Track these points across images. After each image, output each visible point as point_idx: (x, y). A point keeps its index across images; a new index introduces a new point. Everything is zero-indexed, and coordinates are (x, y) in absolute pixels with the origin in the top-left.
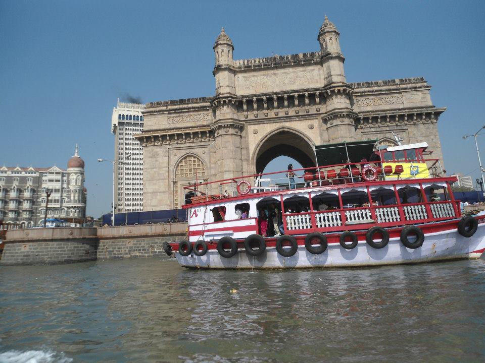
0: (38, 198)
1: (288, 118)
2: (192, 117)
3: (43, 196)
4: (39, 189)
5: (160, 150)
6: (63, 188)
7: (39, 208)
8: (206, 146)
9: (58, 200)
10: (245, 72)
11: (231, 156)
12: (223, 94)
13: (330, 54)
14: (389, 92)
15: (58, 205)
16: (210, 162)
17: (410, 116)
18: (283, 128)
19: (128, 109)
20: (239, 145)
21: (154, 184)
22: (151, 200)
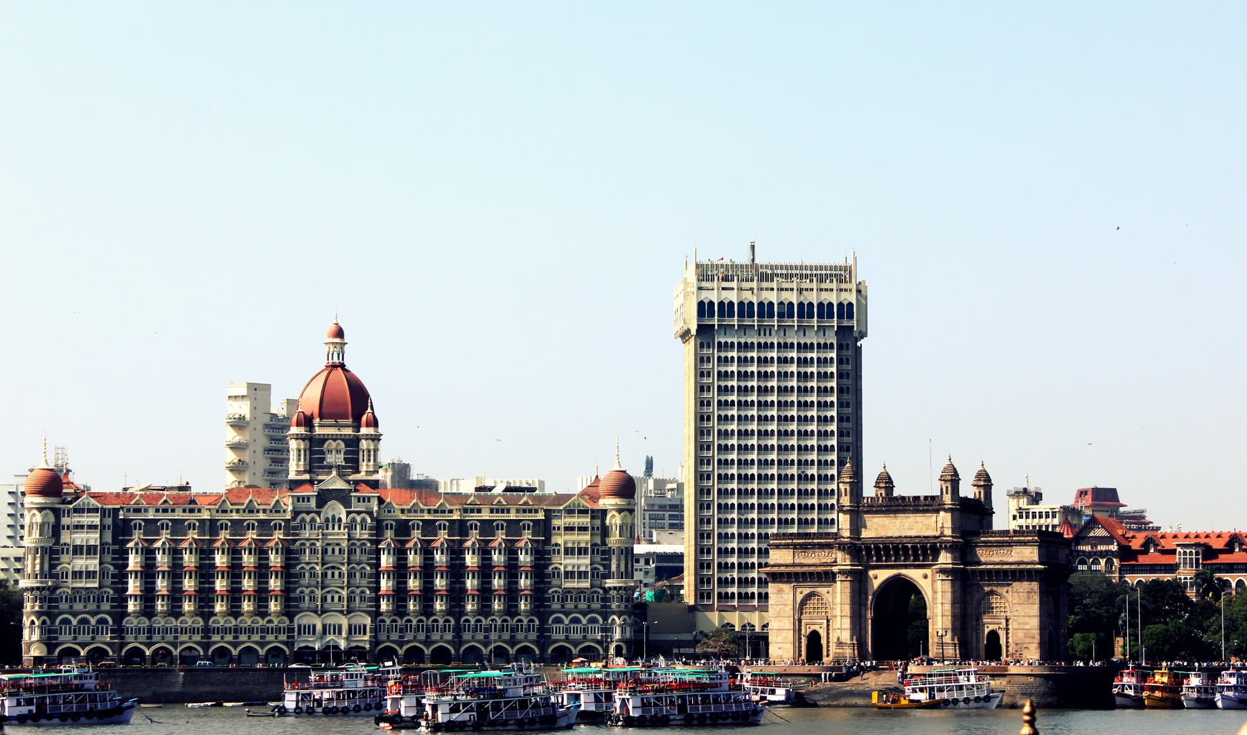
0: (547, 566)
1: (906, 567)
2: (817, 554)
3: (554, 563)
4: (547, 548)
5: (787, 588)
6: (594, 545)
7: (549, 588)
8: (830, 586)
9: (586, 573)
10: (868, 512)
11: (849, 602)
12: (844, 538)
13: (945, 504)
14: (1000, 545)
15: (586, 584)
16: (833, 602)
17: (1013, 572)
18: (900, 575)
19: (725, 284)
20: (858, 590)
21: (780, 621)
22: (777, 637)
